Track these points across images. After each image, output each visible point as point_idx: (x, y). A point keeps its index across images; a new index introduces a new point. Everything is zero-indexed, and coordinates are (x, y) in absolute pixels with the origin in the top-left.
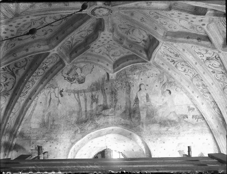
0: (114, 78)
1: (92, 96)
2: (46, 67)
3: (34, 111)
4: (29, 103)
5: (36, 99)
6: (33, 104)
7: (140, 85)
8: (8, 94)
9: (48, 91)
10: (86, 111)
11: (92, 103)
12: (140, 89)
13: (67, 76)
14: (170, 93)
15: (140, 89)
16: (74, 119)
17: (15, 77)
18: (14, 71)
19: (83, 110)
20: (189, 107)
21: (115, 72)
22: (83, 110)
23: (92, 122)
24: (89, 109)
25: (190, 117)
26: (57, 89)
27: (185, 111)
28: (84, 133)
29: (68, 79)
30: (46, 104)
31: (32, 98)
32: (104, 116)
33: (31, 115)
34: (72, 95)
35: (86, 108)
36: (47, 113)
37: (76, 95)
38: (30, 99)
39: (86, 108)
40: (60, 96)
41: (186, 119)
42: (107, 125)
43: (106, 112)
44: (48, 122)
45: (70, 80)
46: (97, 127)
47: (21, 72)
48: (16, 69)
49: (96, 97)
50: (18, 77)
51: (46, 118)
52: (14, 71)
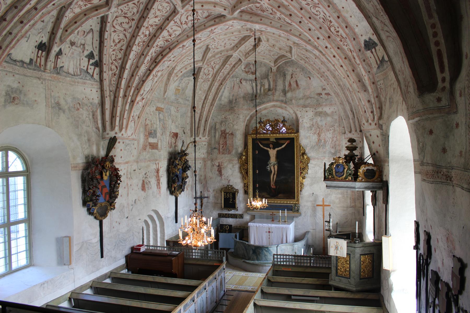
0: (275, 70)
1: (261, 83)
2: (231, 64)
4: (221, 87)
5: (225, 85)
6: (223, 87)
7: (292, 75)
8: (209, 81)
9: (233, 79)
12: (292, 77)
13: (244, 70)
14: (310, 79)
15: (292, 77)
17: (214, 70)
18: (214, 66)
20: (322, 88)
21: (275, 66)
24: (258, 91)
25: (323, 94)
26: (238, 78)
27: (320, 91)
29: (245, 71)
30: (231, 88)
31: (223, 84)
33: (221, 96)
34: (248, 82)
36: (231, 95)
37: (251, 82)
38: (222, 84)
40: (240, 83)
41: (321, 96)
45: (247, 72)
47: (217, 67)
48: (215, 65)
49: (264, 83)
50: (215, 70)
51: (231, 97)
52: (214, 66)
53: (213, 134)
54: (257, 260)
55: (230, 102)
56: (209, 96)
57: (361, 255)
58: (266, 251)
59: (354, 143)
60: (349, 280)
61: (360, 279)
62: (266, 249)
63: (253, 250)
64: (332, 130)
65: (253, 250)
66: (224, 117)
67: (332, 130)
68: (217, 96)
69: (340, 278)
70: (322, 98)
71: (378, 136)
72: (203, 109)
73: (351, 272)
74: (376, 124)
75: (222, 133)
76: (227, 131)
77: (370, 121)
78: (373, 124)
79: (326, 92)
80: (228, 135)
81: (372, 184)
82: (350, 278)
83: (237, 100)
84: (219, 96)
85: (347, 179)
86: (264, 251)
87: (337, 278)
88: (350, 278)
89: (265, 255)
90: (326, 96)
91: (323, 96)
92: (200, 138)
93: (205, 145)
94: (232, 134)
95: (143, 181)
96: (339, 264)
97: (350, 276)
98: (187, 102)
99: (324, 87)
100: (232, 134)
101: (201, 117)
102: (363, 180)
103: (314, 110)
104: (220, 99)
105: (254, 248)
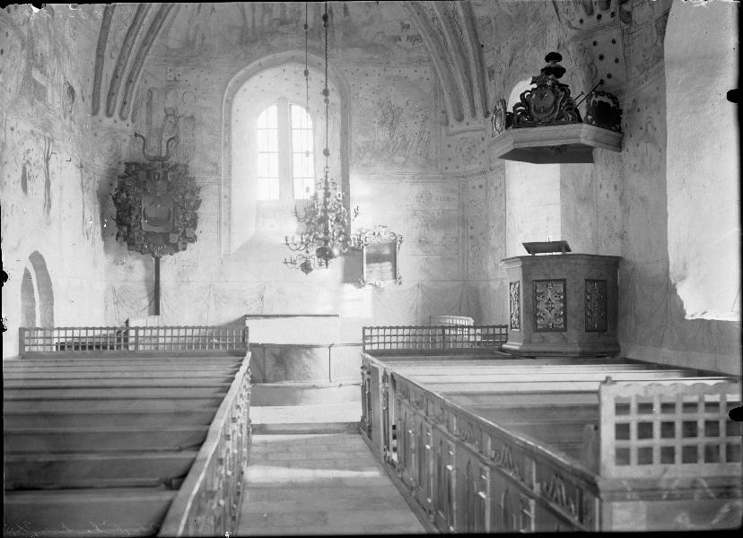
3: (176, 20)
10: (253, 27)
11: (263, 16)
16: (235, 38)
19: (250, 25)
20: (402, 23)
22: (250, 25)
23: (263, 43)
24: (258, 23)
25: (403, 39)
28: (249, 58)
32: (282, 34)
33: (170, 26)
35: (254, 23)
39: (254, 23)
41: (398, 43)
42: (285, 47)
43: (283, 29)
44: (194, 41)
46: (270, 50)
51: (192, 32)
53: (144, 117)
54: (287, 379)
55: (188, 43)
56: (145, 16)
57: (586, 280)
58: (307, 356)
59: (558, 63)
60: (564, 333)
61: (587, 331)
62: (308, 352)
63: (274, 355)
64: (419, 115)
65: (274, 355)
66: (172, 79)
67: (419, 115)
68: (160, 21)
69: (543, 334)
70: (400, 47)
71: (614, 42)
72: (128, 49)
73: (569, 317)
74: (613, 15)
75: (167, 116)
76: (181, 112)
77: (597, 11)
78: (606, 17)
79: (411, 32)
80: (181, 119)
81: (606, 135)
82: (565, 330)
83: (207, 41)
84: (166, 22)
85: (563, 120)
86: (303, 356)
87: (537, 334)
88: (565, 330)
89: (305, 366)
90: (410, 45)
91: (404, 42)
92: (115, 122)
93: (125, 140)
94: (192, 117)
95: (24, 169)
96: (541, 306)
97: (566, 326)
98: (92, 22)
99: (406, 22)
100: (192, 117)
101: (121, 68)
102: (594, 123)
103: (382, 73)
104: (166, 32)
105: (277, 352)
